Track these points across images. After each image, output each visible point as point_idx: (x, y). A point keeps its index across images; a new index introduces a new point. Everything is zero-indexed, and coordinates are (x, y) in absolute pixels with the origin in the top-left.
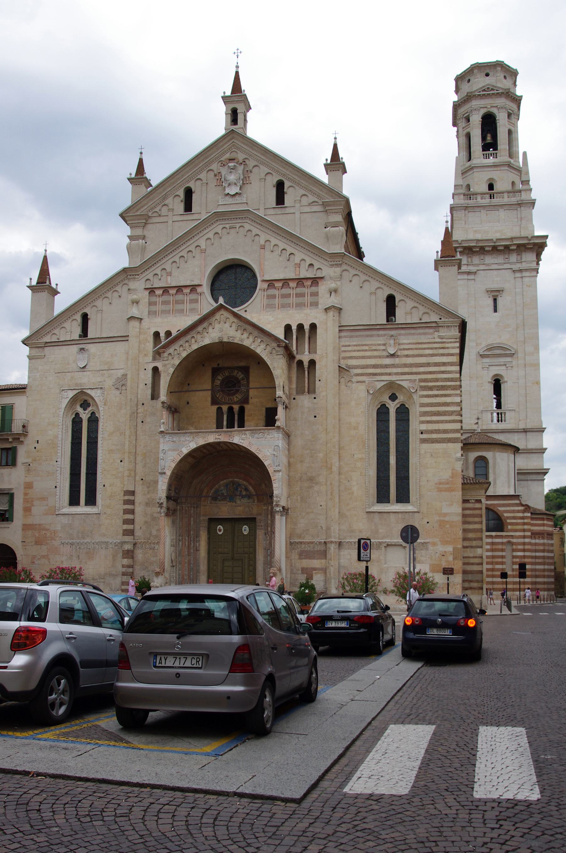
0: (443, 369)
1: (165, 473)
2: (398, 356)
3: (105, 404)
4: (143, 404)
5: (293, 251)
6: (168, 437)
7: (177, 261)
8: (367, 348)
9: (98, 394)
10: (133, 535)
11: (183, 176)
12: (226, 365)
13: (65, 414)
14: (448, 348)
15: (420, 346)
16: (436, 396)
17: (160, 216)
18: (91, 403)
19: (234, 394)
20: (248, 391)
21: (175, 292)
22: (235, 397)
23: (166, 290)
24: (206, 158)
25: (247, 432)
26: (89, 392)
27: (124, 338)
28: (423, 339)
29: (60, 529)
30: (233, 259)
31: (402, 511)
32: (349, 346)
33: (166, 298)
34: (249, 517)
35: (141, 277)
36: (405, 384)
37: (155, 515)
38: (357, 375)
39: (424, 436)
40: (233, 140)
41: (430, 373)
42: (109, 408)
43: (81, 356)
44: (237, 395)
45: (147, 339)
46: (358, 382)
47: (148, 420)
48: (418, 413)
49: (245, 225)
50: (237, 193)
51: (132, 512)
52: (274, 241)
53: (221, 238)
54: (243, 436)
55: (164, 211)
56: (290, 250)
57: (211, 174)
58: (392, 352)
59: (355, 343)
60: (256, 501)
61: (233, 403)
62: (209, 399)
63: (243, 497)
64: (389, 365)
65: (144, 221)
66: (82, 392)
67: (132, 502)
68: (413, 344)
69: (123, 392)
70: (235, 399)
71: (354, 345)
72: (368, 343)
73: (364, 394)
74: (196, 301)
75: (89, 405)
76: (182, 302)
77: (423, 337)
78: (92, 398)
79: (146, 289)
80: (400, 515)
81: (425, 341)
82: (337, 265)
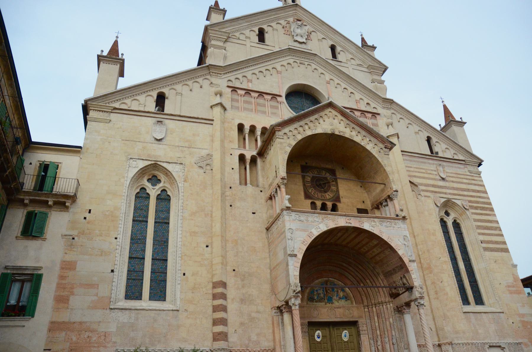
0: (478, 194)
1: (295, 256)
2: (447, 181)
3: (185, 181)
4: (231, 188)
5: (353, 91)
6: (293, 214)
7: (257, 73)
8: (424, 171)
9: (177, 170)
10: (227, 341)
11: (258, 19)
12: (314, 165)
13: (131, 185)
14: (476, 180)
15: (459, 176)
16: (481, 214)
17: (239, 39)
18: (163, 180)
19: (325, 192)
20: (338, 191)
21: (257, 96)
22: (326, 194)
23: (248, 92)
24: (276, 14)
25: (376, 220)
26: (165, 165)
27: (209, 121)
28: (459, 171)
29: (114, 330)
30: (305, 85)
31: (491, 311)
32: (411, 167)
33: (247, 98)
34: (351, 320)
35: (223, 77)
36: (458, 202)
37: (254, 315)
38: (423, 191)
39: (484, 245)
40: (296, 11)
41: (472, 196)
42: (190, 186)
43: (158, 128)
44: (328, 193)
45: (231, 128)
46: (425, 196)
47: (238, 204)
48: (474, 226)
49: (312, 64)
50: (303, 42)
51: (224, 309)
52: (337, 81)
53: (293, 68)
54: (373, 223)
55: (242, 37)
56: (350, 90)
57: (281, 27)
58: (444, 177)
59: (415, 166)
60: (354, 303)
61: (325, 200)
62: (302, 193)
63: (340, 298)
64: (443, 187)
65: (226, 38)
66: (155, 166)
67: (223, 296)
68: (454, 173)
69: (207, 171)
70: (327, 196)
71: (415, 168)
72: (423, 167)
73: (433, 206)
74: (277, 108)
75: (159, 181)
76: (264, 106)
77: (458, 170)
78: (167, 173)
79: (228, 87)
80: (490, 315)
81: (461, 173)
82: (388, 108)
